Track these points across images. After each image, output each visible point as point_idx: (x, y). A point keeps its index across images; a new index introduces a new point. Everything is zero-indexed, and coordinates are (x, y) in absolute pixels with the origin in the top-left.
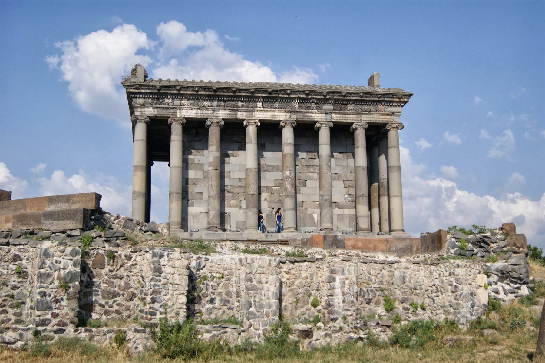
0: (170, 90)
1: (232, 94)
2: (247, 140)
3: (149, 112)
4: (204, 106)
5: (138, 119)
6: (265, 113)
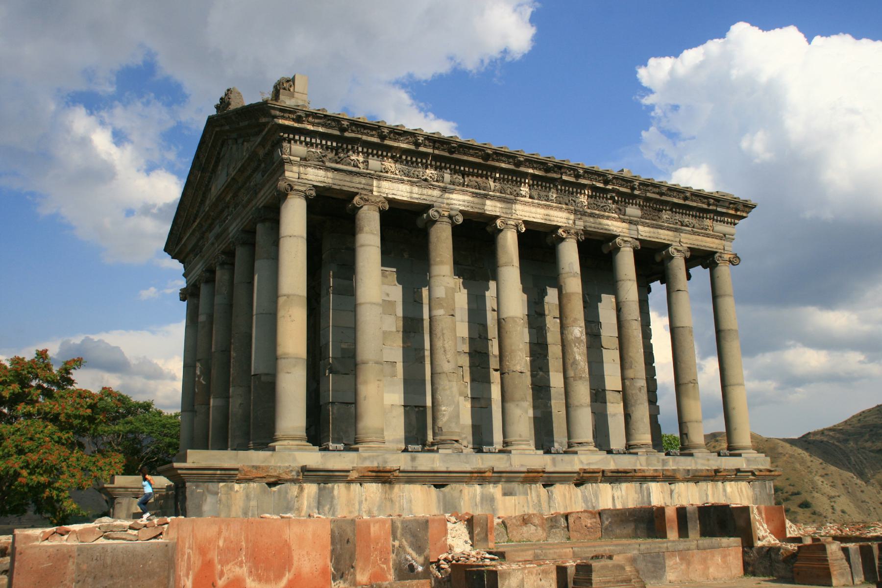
0: (367, 134)
1: (481, 161)
2: (502, 258)
3: (317, 176)
4: (426, 180)
5: (292, 189)
6: (533, 209)
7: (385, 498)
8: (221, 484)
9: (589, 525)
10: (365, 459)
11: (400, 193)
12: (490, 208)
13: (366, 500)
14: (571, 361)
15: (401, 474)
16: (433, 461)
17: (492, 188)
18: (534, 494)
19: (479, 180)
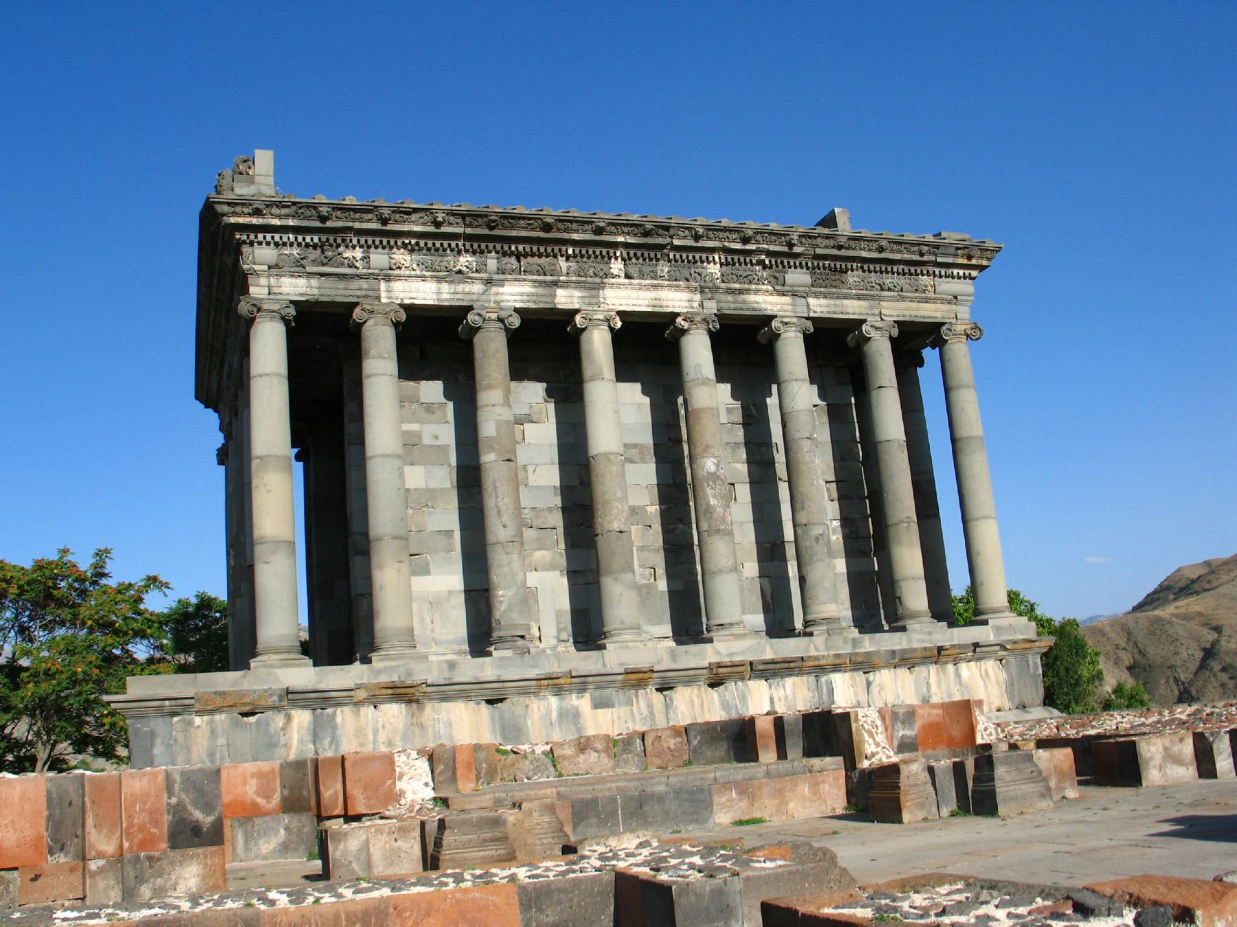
2: (588, 371)
3: (295, 288)
4: (460, 272)
5: (259, 310)
6: (634, 294)
7: (412, 724)
8: (176, 719)
9: (672, 747)
10: (379, 672)
11: (420, 295)
12: (563, 300)
13: (383, 727)
14: (704, 507)
15: (430, 689)
16: (482, 667)
17: (564, 270)
18: (642, 704)
19: (543, 260)
